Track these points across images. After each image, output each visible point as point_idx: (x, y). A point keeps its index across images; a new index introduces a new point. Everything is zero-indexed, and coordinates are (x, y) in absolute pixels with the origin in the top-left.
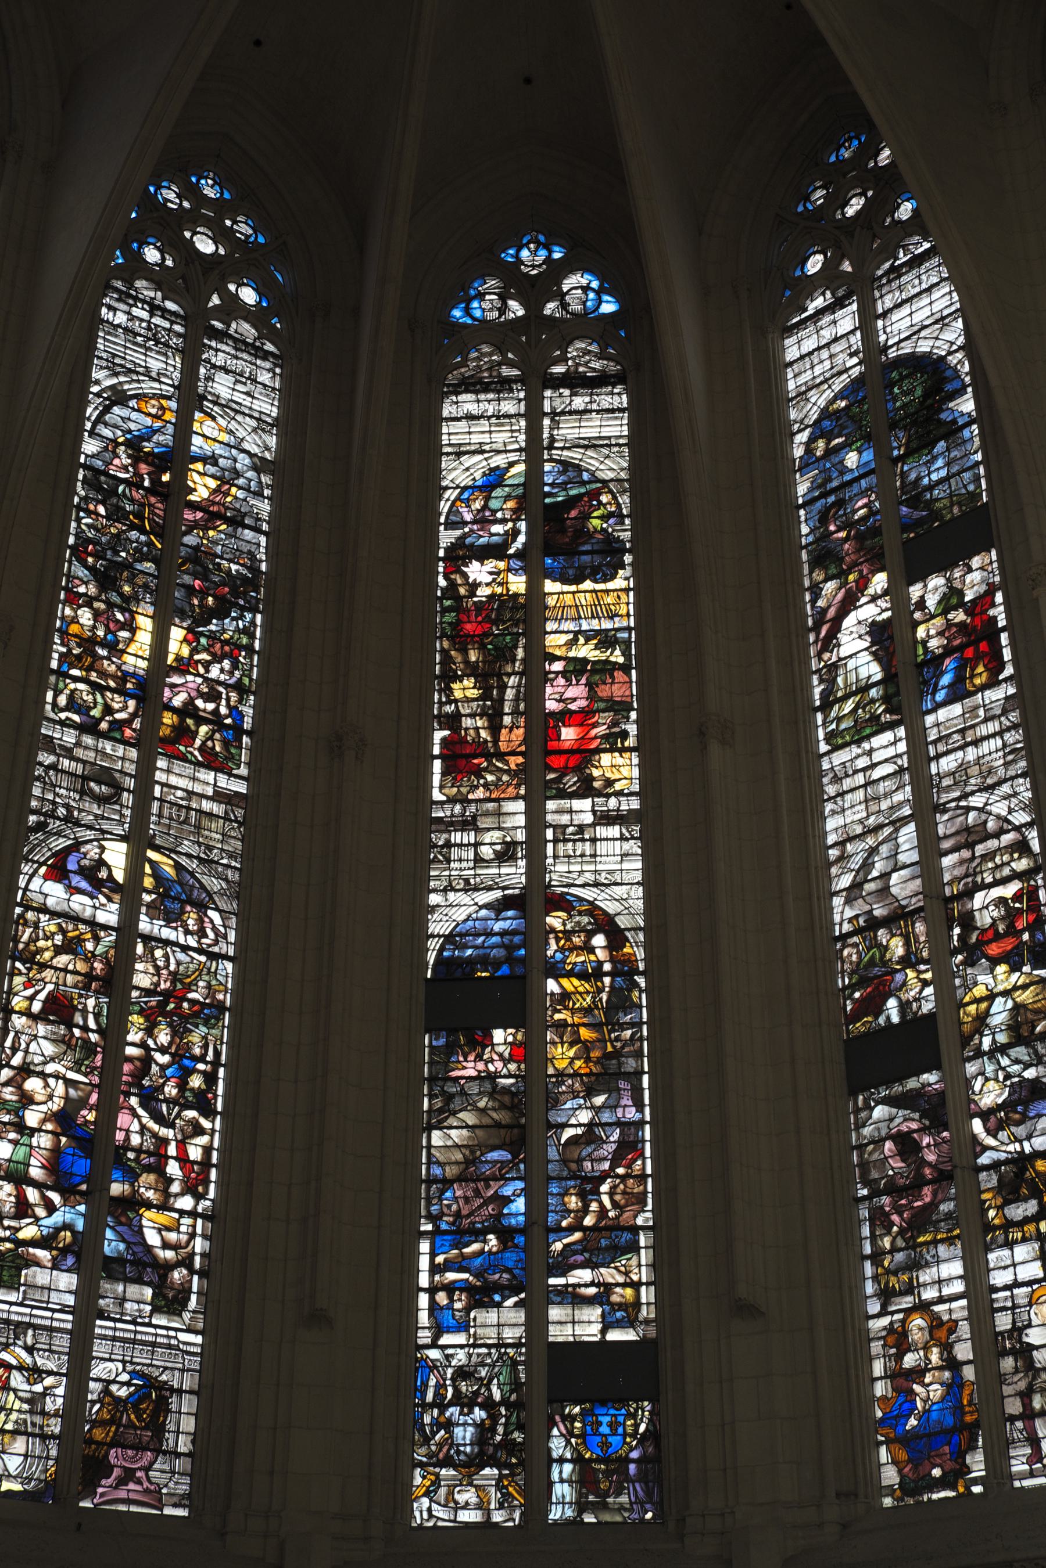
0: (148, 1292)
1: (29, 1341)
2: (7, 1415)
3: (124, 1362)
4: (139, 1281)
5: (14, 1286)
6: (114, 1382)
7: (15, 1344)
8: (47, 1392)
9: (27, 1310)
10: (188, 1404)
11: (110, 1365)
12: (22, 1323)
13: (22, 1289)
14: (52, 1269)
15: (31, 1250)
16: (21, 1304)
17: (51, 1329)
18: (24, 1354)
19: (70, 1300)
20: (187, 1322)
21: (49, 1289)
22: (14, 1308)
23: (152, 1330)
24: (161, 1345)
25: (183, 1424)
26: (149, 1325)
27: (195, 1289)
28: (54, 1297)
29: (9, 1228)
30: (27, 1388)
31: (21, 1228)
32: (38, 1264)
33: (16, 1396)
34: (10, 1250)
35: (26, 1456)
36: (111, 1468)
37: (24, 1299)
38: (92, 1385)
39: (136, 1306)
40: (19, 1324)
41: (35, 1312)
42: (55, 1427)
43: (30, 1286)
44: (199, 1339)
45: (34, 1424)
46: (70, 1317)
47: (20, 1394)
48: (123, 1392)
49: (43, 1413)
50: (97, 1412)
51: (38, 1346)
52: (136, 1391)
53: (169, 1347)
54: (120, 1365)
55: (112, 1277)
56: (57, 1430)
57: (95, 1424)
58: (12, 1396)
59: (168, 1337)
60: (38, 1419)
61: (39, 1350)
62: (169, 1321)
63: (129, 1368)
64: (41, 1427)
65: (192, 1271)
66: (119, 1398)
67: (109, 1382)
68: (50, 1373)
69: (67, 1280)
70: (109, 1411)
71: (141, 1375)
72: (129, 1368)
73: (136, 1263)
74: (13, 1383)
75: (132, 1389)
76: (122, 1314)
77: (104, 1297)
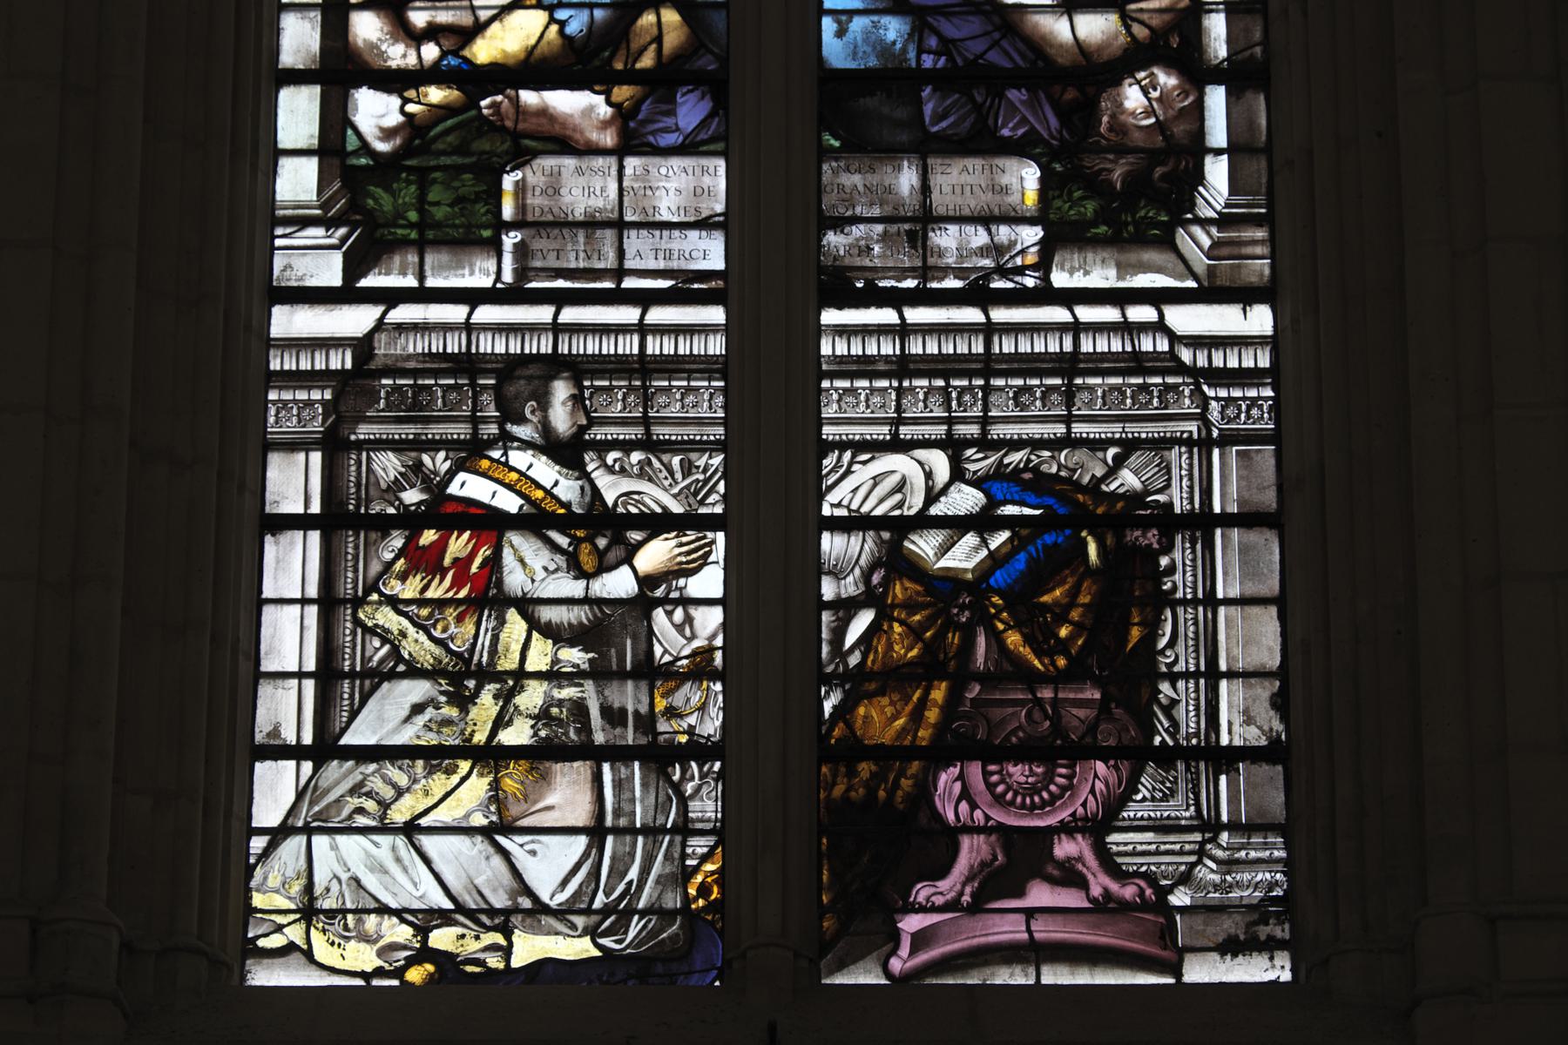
0: (1025, 180)
1: (561, 418)
2: (506, 697)
3: (953, 447)
4: (983, 142)
5: (478, 235)
6: (923, 521)
7: (506, 439)
8: (654, 592)
9: (543, 313)
10: (1240, 566)
11: (898, 463)
12: (524, 360)
13: (510, 240)
14: (621, 151)
15: (528, 97)
16: (514, 295)
17: (644, 367)
18: (545, 471)
19: (710, 253)
20: (1200, 261)
21: (620, 225)
22: (487, 314)
23: (1059, 314)
24: (1100, 364)
25: (1232, 643)
26: (1046, 295)
27: (1218, 134)
28: (641, 250)
29: (433, 32)
30: (576, 588)
31: (479, 28)
32: (562, 140)
33: (534, 624)
34: (444, 110)
35: (596, 832)
36: (950, 837)
37: (522, 273)
38: (832, 544)
39: (979, 237)
40: (510, 366)
41: (570, 315)
42: (703, 713)
43: (539, 225)
44: (1260, 320)
45: (614, 716)
46: (715, 314)
47: (548, 614)
48: (964, 556)
49: (649, 672)
50: (866, 639)
51: (599, 433)
52: (1014, 545)
53: (1137, 363)
54: (939, 462)
55: (872, 147)
56: (711, 726)
57: (859, 685)
58: (516, 626)
59: (1127, 328)
60: (629, 697)
61: (603, 447)
62: (1123, 269)
63: (978, 463)
64: (646, 722)
65: (1197, 73)
66: (951, 579)
67: (902, 526)
68: (658, 524)
69: (686, 184)
70: (915, 633)
71: (1033, 483)
72: (978, 463)
73: (961, 78)
74: (514, 580)
75: (999, 539)
76: (925, 272)
77: (840, 224)
